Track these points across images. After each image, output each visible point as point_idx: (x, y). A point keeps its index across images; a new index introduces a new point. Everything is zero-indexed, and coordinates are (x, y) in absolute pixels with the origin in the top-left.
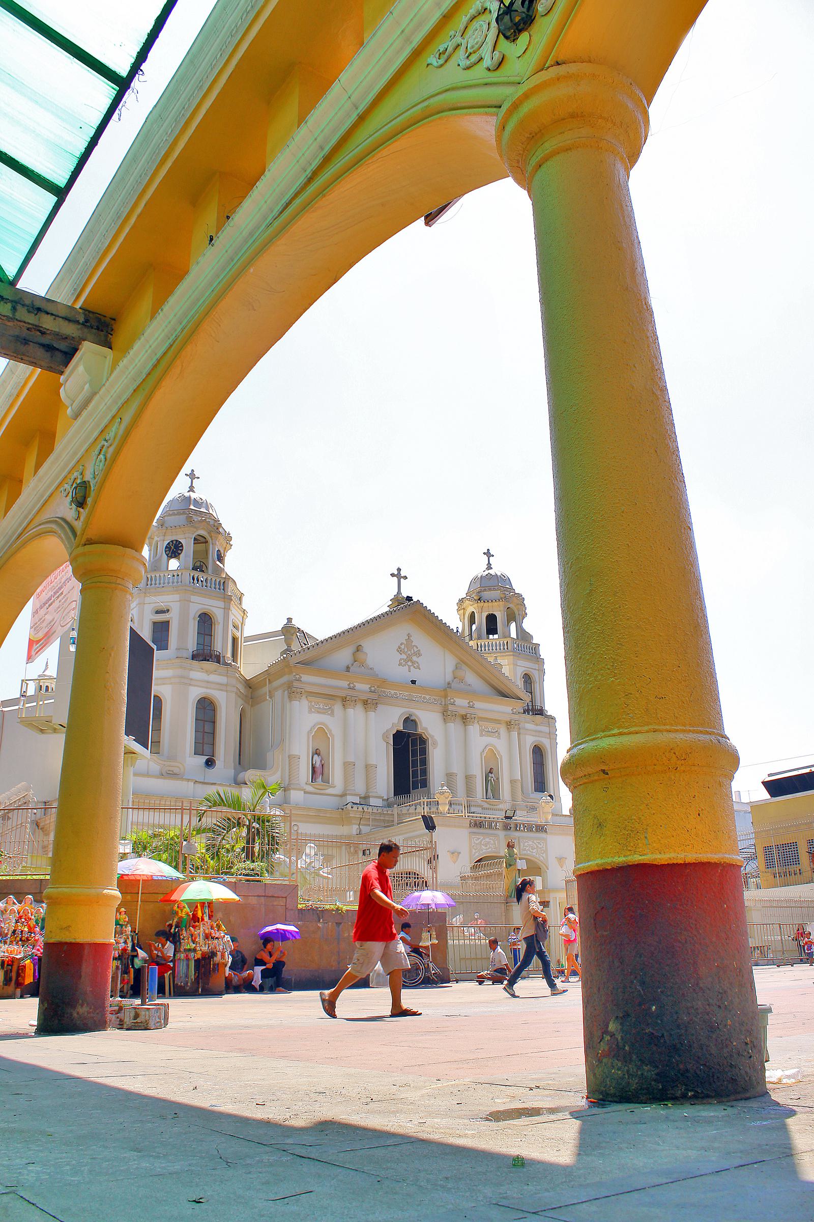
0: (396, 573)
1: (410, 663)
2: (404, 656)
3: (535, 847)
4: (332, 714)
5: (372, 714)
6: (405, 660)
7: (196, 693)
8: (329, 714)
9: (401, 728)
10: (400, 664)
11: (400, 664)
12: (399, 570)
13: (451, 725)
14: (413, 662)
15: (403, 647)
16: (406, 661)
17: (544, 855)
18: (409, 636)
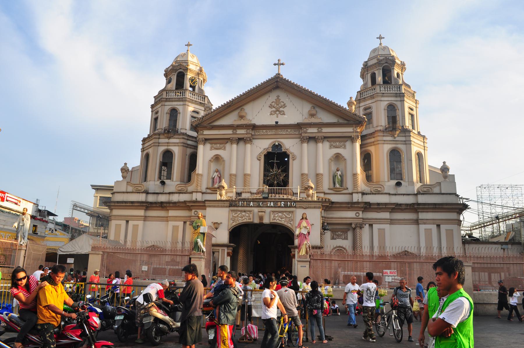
0: (277, 62)
1: (278, 113)
2: (274, 109)
3: (284, 217)
4: (225, 149)
5: (248, 146)
6: (275, 112)
7: (162, 149)
8: (223, 149)
9: (271, 151)
10: (271, 114)
11: (271, 114)
12: (279, 60)
13: (305, 145)
14: (280, 112)
15: (273, 104)
16: (275, 112)
17: (292, 222)
18: (278, 97)
